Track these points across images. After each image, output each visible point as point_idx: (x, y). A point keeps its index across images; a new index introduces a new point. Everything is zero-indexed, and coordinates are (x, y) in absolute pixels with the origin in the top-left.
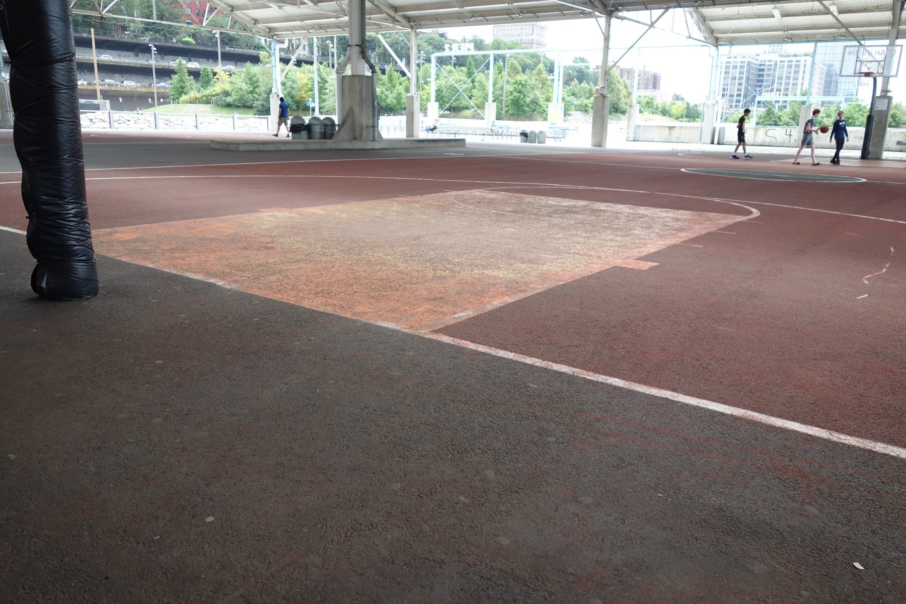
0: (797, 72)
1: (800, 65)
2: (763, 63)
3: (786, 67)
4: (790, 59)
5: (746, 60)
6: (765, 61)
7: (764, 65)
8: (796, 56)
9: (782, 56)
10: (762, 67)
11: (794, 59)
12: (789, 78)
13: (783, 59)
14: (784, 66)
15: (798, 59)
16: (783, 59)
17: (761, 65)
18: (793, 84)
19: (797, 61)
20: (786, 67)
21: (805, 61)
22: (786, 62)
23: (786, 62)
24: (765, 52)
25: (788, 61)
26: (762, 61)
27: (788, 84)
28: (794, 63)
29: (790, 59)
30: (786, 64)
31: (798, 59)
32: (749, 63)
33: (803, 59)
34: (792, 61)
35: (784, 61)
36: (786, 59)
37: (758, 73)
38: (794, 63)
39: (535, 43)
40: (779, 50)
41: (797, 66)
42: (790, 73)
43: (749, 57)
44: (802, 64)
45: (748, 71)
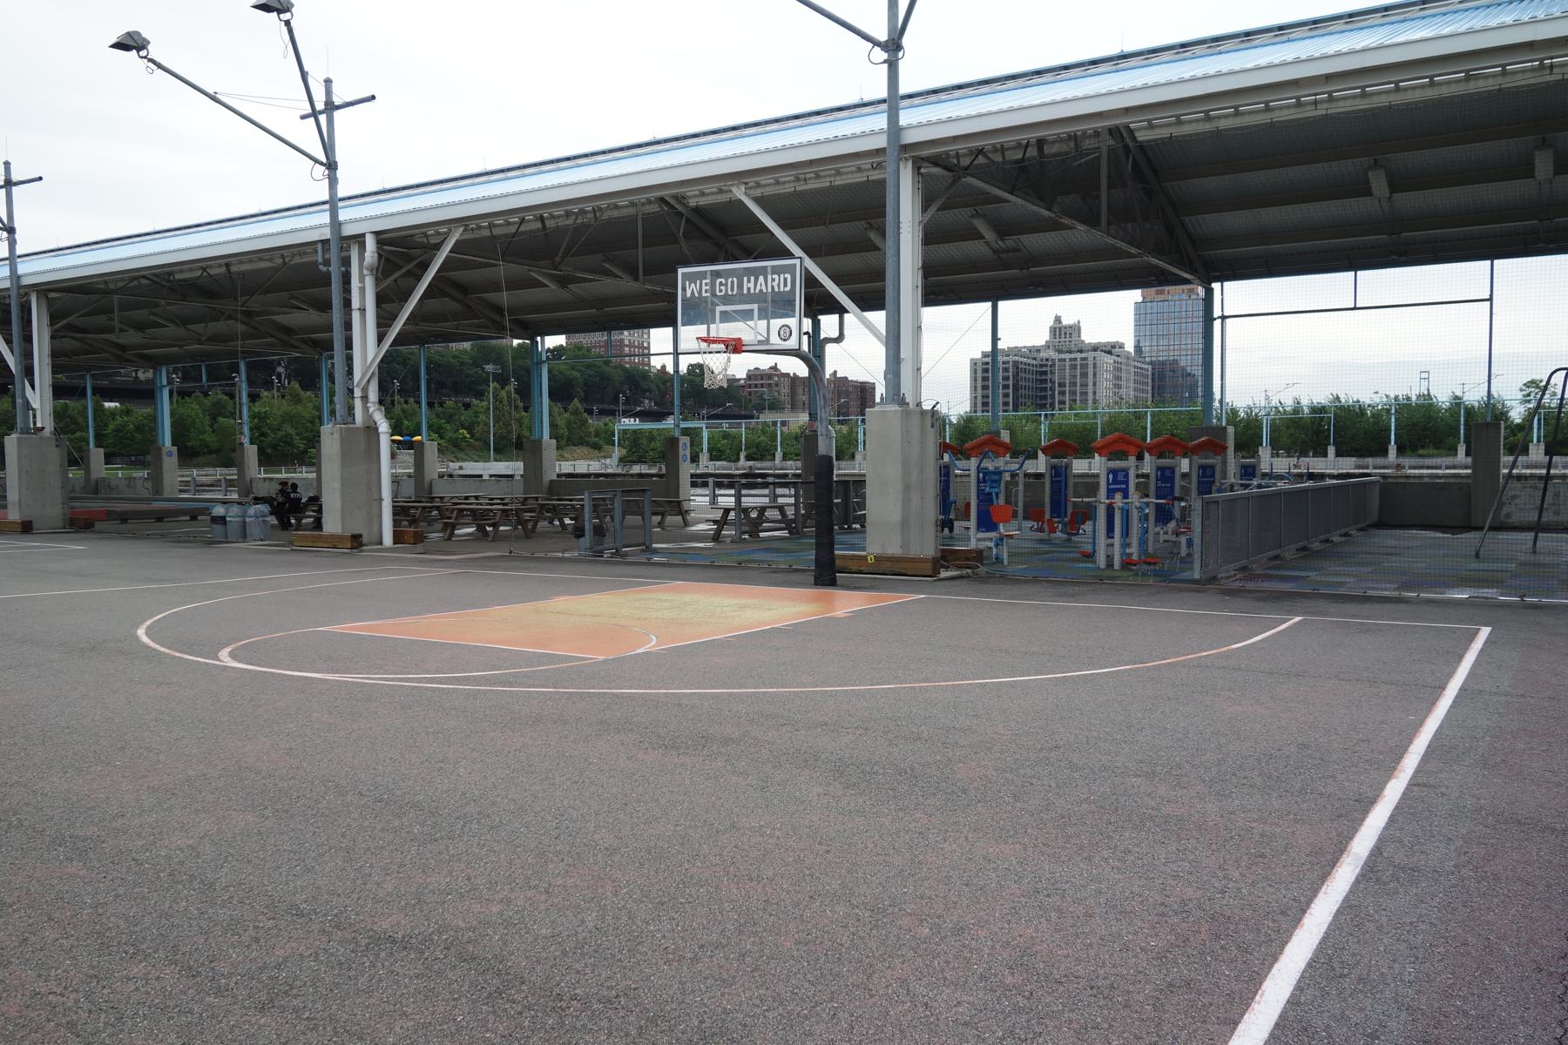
0: (1084, 375)
1: (1087, 364)
2: (1044, 362)
3: (1067, 367)
4: (1073, 356)
5: (1012, 358)
6: (1047, 360)
7: (1046, 365)
8: (1081, 351)
9: (1060, 352)
10: (1044, 369)
11: (1079, 355)
12: (1074, 384)
13: (1063, 356)
14: (1065, 366)
15: (1083, 355)
16: (1063, 356)
17: (1041, 366)
18: (1081, 393)
19: (1083, 359)
20: (1067, 367)
21: (1094, 358)
22: (1067, 360)
23: (1067, 360)
24: (1049, 347)
25: (1071, 360)
26: (1042, 360)
27: (1074, 393)
28: (1079, 362)
29: (1073, 356)
30: (1067, 363)
31: (1083, 355)
32: (1016, 363)
33: (1092, 354)
34: (1075, 359)
35: (1064, 360)
36: (1067, 356)
37: (1039, 377)
38: (1079, 362)
39: (627, 346)
40: (1067, 343)
41: (1084, 366)
42: (1075, 376)
43: (1016, 355)
44: (1091, 359)
45: (1016, 376)
